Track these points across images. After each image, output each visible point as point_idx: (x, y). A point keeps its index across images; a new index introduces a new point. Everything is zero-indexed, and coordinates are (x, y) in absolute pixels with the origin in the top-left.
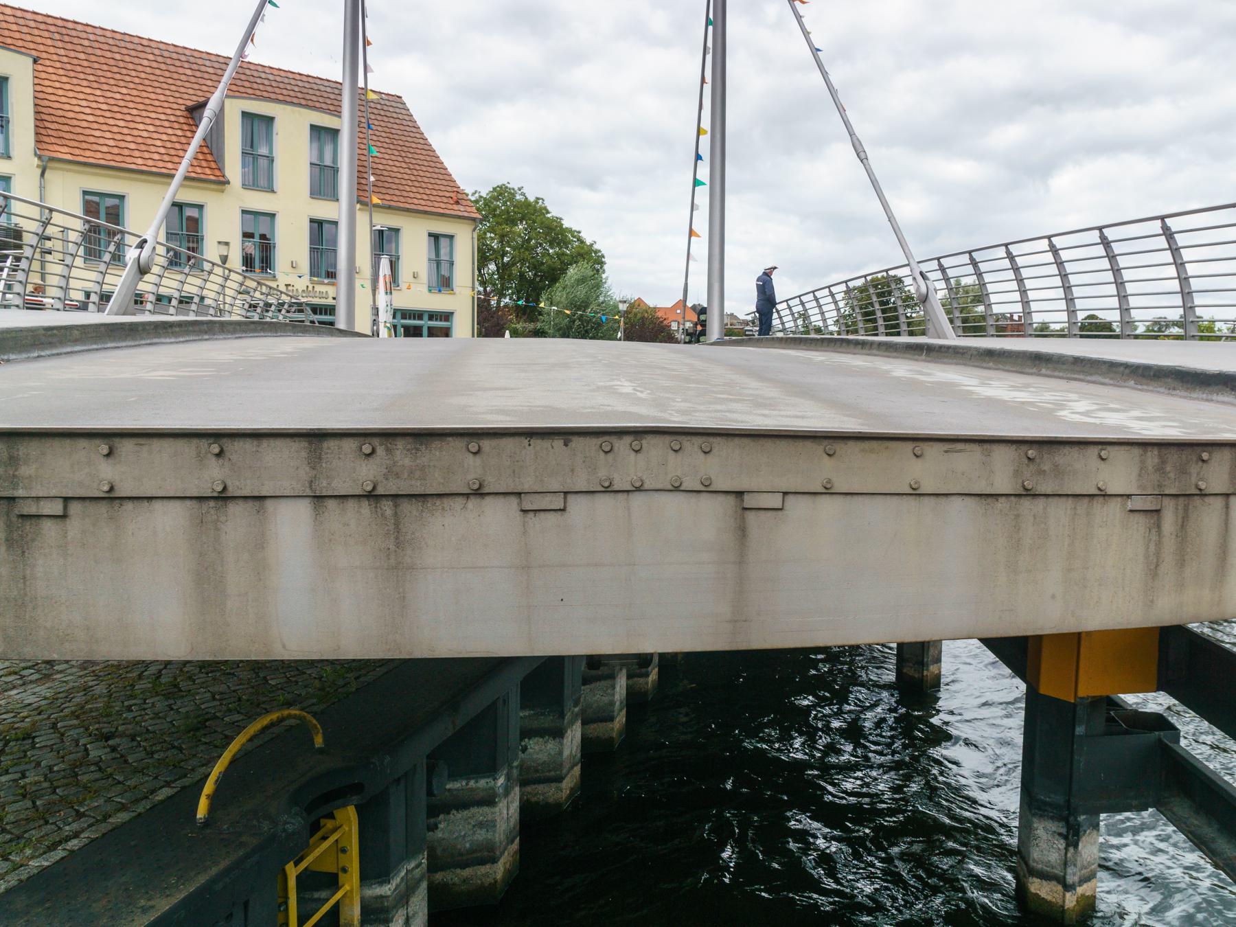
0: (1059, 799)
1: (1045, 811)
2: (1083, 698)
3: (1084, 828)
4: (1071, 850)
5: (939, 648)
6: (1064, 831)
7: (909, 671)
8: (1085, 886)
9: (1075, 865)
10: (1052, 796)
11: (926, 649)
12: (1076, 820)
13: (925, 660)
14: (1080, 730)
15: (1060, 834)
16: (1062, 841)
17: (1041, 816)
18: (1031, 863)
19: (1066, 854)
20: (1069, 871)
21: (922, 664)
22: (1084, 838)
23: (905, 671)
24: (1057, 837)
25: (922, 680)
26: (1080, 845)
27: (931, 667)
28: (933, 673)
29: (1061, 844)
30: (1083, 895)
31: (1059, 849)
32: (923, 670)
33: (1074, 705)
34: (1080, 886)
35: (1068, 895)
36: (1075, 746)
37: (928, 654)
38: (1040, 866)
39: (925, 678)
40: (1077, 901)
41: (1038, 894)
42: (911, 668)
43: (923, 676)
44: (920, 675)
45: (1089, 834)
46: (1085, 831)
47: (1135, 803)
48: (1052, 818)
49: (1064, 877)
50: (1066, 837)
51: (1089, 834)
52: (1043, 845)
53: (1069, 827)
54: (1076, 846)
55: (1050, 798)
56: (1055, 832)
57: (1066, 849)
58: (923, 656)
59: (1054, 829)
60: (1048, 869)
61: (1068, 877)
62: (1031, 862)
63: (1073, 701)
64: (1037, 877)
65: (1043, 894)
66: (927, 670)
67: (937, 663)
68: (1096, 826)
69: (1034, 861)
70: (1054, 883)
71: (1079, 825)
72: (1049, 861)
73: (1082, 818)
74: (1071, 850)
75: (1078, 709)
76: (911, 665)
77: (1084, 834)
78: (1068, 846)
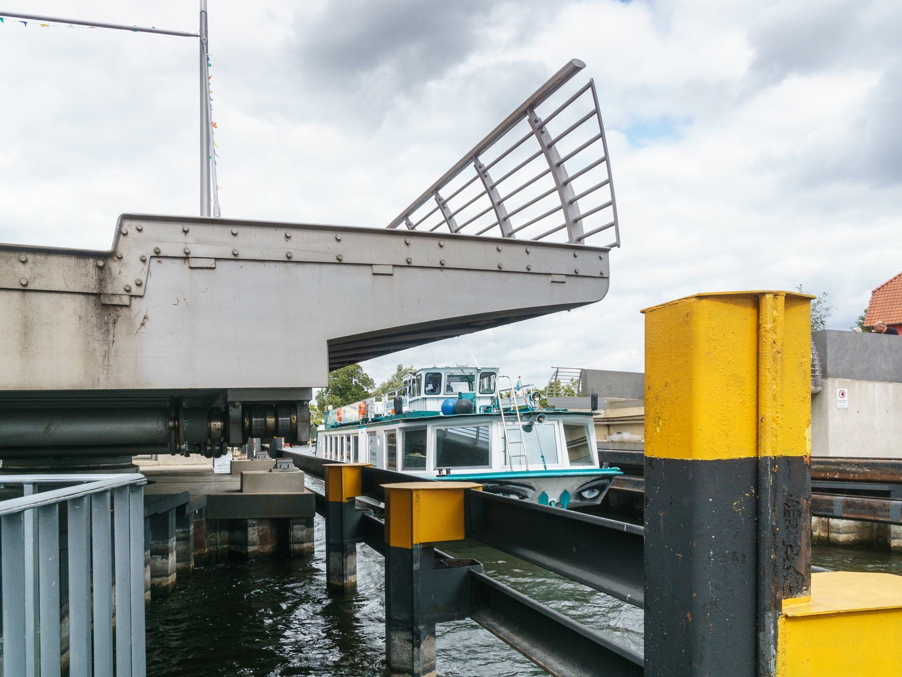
0: (405, 616)
1: (399, 626)
2: (417, 544)
3: (424, 634)
5: (354, 564)
6: (410, 637)
7: (334, 582)
9: (419, 660)
10: (402, 615)
11: (344, 564)
12: (417, 627)
13: (345, 572)
14: (416, 566)
15: (408, 640)
16: (410, 645)
17: (396, 630)
18: (393, 665)
19: (413, 653)
20: (415, 664)
21: (342, 576)
22: (424, 642)
23: (331, 582)
24: (406, 642)
25: (343, 586)
26: (422, 646)
27: (349, 577)
28: (351, 581)
29: (409, 647)
31: (408, 651)
32: (343, 580)
33: (412, 550)
34: (423, 675)
36: (414, 577)
37: (346, 568)
38: (397, 665)
39: (345, 585)
42: (336, 579)
43: (343, 584)
44: (342, 584)
46: (425, 637)
47: (456, 614)
48: (403, 630)
49: (413, 670)
50: (411, 641)
51: (428, 639)
52: (398, 650)
53: (413, 633)
54: (419, 647)
55: (400, 616)
56: (405, 639)
58: (343, 571)
59: (405, 637)
61: (415, 669)
62: (392, 663)
63: (410, 548)
64: (396, 673)
67: (354, 575)
68: (433, 634)
69: (394, 662)
71: (419, 631)
72: (403, 661)
73: (421, 627)
74: (416, 649)
75: (414, 552)
76: (335, 577)
77: (424, 639)
78: (413, 647)
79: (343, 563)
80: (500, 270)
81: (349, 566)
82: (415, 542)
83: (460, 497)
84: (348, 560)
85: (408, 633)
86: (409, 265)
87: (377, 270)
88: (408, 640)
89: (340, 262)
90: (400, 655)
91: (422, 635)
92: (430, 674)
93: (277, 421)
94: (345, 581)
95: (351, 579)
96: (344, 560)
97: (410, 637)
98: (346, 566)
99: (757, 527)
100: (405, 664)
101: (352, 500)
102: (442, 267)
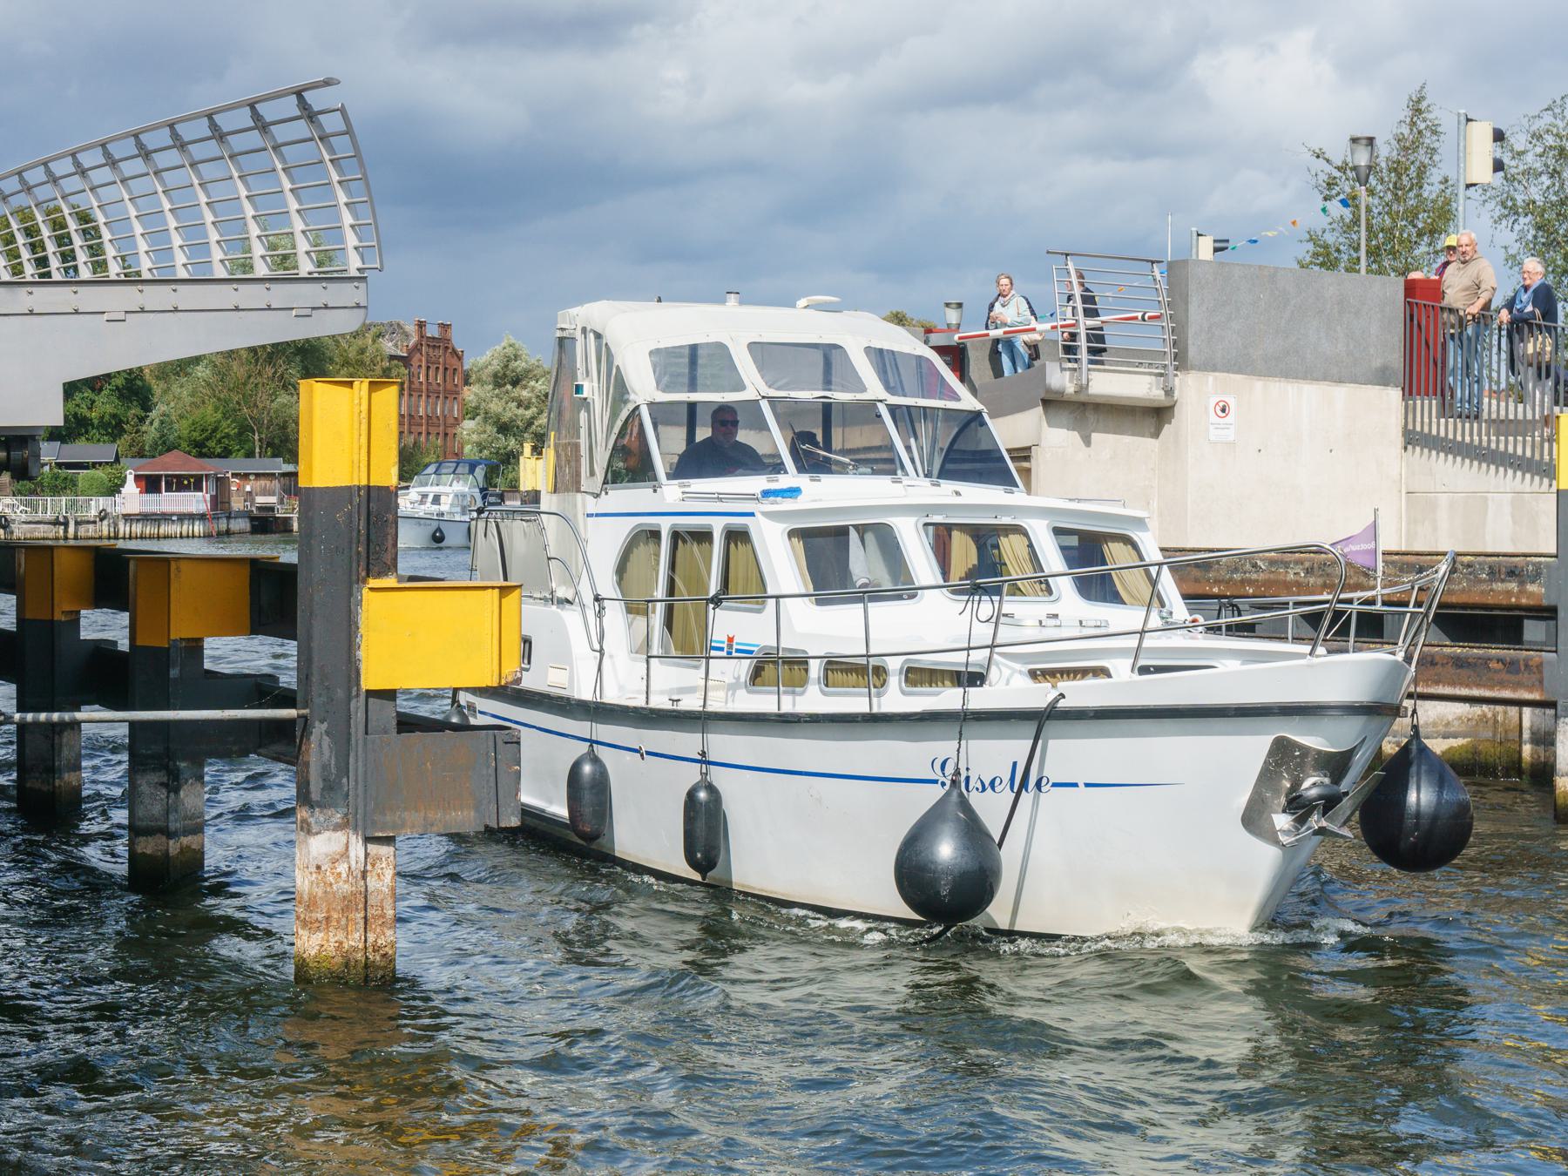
4: (172, 795)
7: (32, 783)
9: (176, 811)
11: (57, 747)
14: (174, 673)
15: (162, 784)
17: (144, 771)
20: (171, 817)
21: (51, 770)
25: (54, 792)
26: (182, 793)
27: (66, 776)
29: (162, 794)
30: (188, 847)
33: (168, 649)
37: (59, 755)
43: (54, 787)
46: (187, 781)
48: (154, 770)
52: (147, 801)
57: (168, 797)
66: (60, 778)
69: (140, 819)
70: (158, 835)
71: (178, 769)
74: (172, 795)
76: (37, 775)
79: (53, 745)
80: (237, 309)
81: (65, 752)
82: (172, 637)
83: (246, 571)
84: (65, 740)
85: (162, 774)
88: (162, 784)
89: (77, 312)
93: (9, 455)
94: (57, 782)
95: (71, 778)
96: (56, 737)
97: (165, 780)
98: (60, 751)
100: (156, 820)
101: (73, 617)
102: (176, 310)
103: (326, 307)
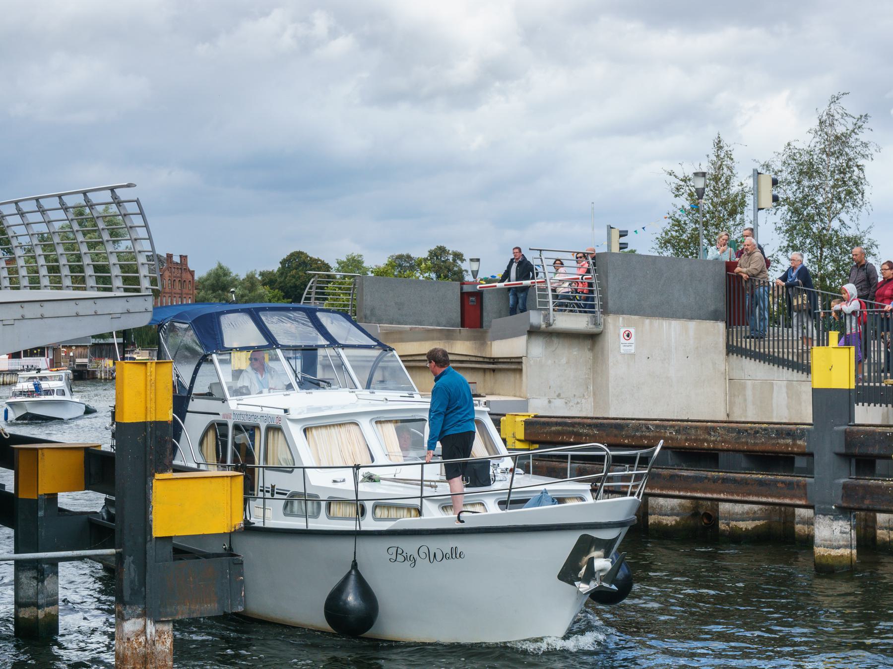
4: (40, 584)
8: (50, 608)
9: (43, 593)
12: (41, 566)
14: (41, 513)
15: (34, 578)
16: (35, 581)
17: (23, 570)
20: (40, 597)
22: (48, 579)
26: (45, 583)
30: (49, 613)
31: (34, 586)
33: (37, 500)
35: (40, 611)
40: (45, 615)
41: (23, 617)
45: (51, 577)
46: (48, 575)
48: (29, 570)
49: (37, 602)
51: (51, 577)
52: (25, 587)
53: (38, 571)
54: (43, 581)
57: (37, 585)
59: (30, 575)
60: (28, 600)
63: (36, 498)
65: (26, 616)
69: (21, 598)
70: (32, 607)
78: (38, 582)
82: (40, 493)
83: (81, 455)
85: (32, 572)
86: (23, 318)
87: (5, 323)
88: (34, 578)
90: (27, 591)
91: (45, 573)
92: (53, 607)
97: (35, 575)
99: (146, 447)
100: (31, 598)
103: (128, 312)
